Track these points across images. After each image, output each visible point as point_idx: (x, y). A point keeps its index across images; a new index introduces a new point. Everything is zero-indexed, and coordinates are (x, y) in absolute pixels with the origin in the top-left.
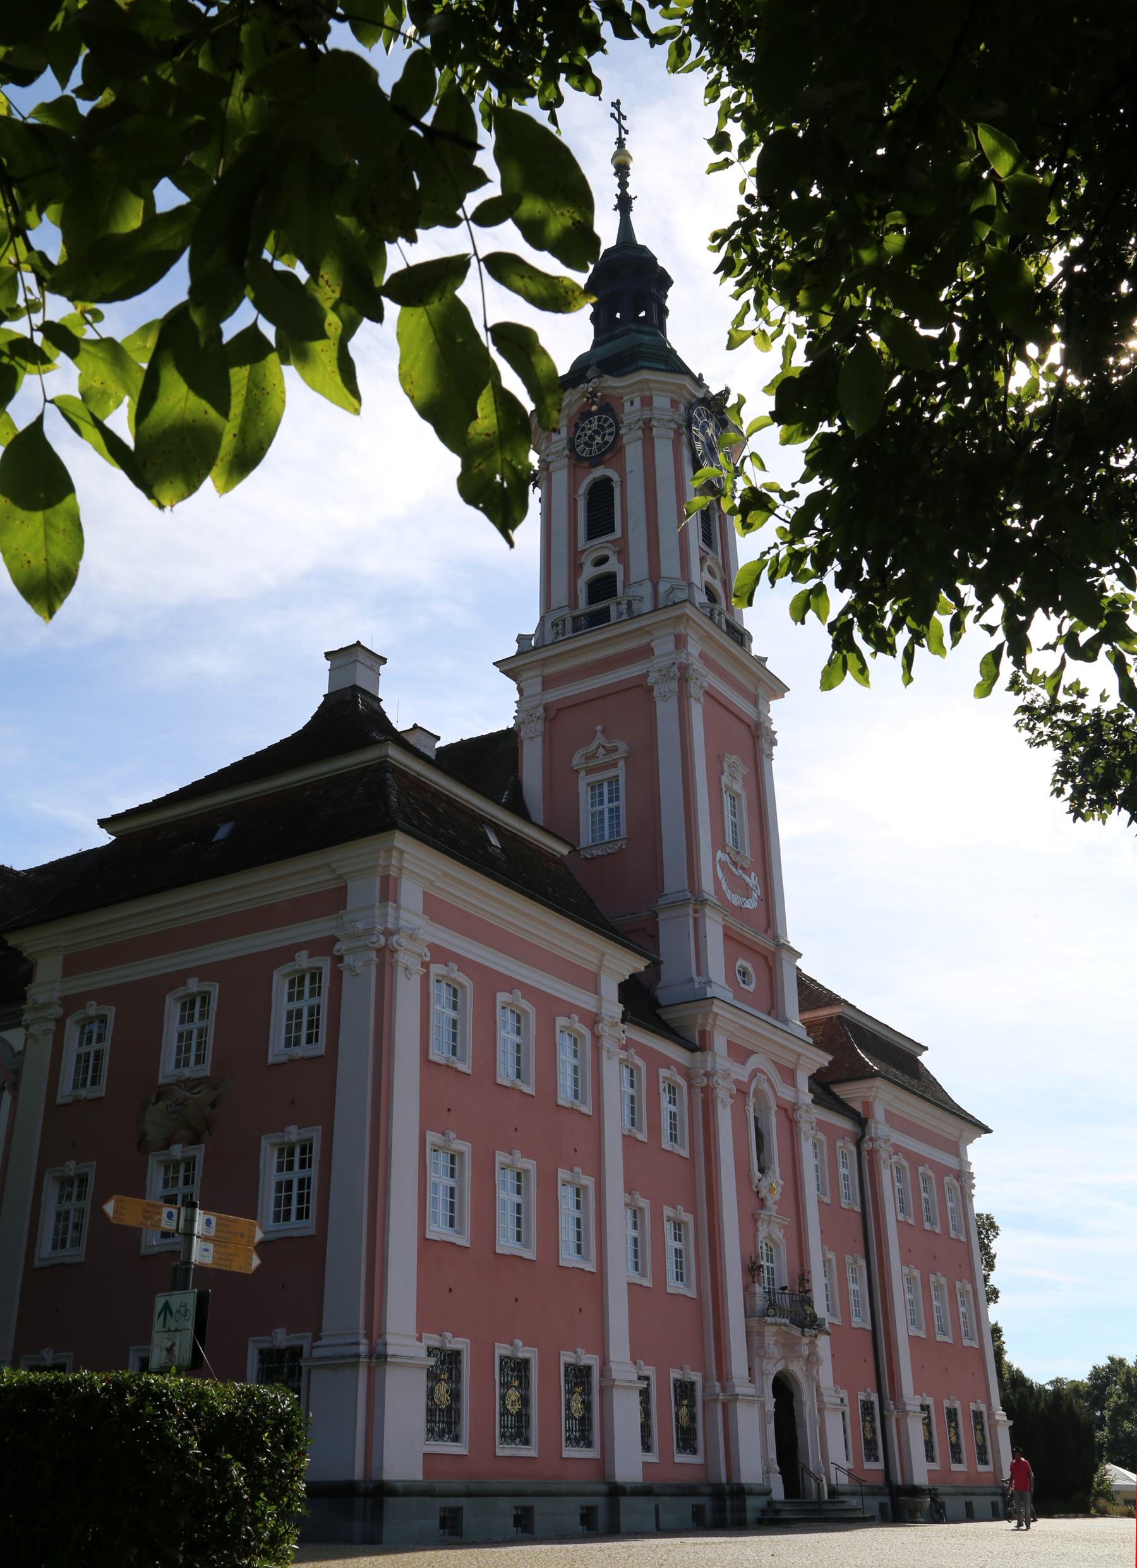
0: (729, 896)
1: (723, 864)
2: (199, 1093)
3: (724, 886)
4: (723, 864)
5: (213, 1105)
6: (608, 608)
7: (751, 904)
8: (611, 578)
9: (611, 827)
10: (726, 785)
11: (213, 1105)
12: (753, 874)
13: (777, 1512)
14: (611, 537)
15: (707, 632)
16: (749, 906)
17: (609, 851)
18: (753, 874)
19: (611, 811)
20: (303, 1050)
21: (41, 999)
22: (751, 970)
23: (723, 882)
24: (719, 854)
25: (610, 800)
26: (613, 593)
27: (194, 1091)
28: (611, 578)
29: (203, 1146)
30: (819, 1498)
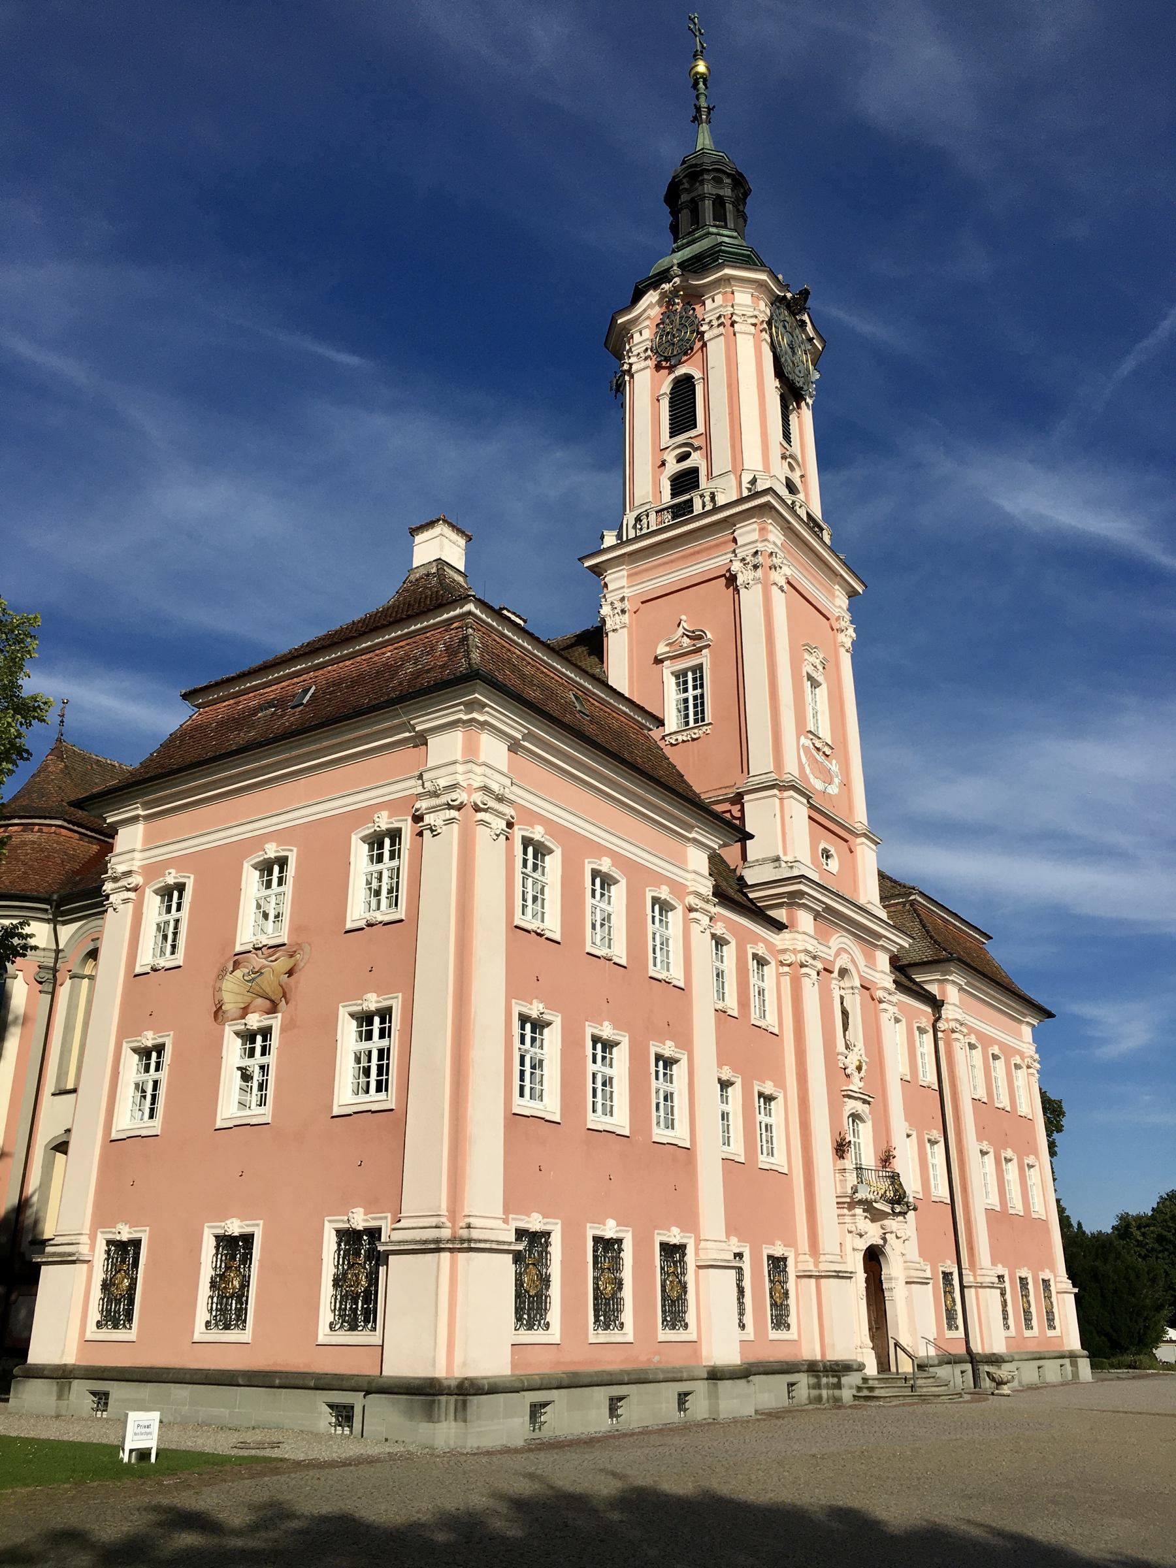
0: (812, 781)
1: (806, 749)
2: (276, 960)
3: (808, 771)
4: (806, 749)
5: (290, 973)
6: (691, 500)
7: (833, 790)
8: (694, 471)
9: (696, 714)
10: (808, 673)
11: (290, 973)
12: (834, 762)
13: (871, 1389)
14: (692, 433)
15: (789, 522)
16: (831, 792)
17: (694, 736)
18: (834, 762)
19: (695, 698)
20: (385, 914)
21: (121, 869)
22: (833, 851)
23: (806, 766)
24: (803, 740)
25: (695, 688)
26: (695, 485)
27: (271, 959)
28: (694, 471)
29: (279, 1015)
30: (918, 1378)
